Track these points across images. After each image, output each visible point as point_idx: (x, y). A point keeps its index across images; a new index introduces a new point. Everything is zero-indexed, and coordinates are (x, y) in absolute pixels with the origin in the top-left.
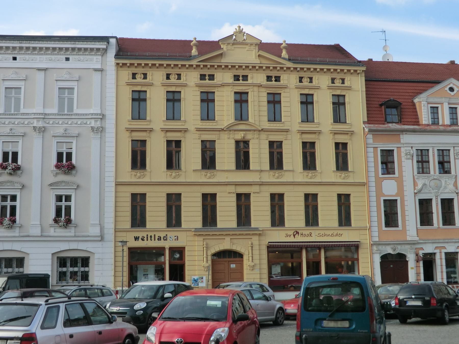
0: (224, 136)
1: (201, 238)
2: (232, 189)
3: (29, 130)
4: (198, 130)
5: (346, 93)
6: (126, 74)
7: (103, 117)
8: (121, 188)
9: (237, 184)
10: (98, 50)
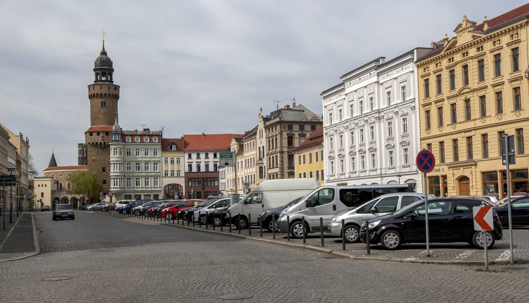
0: (458, 99)
1: (451, 169)
2: (463, 134)
3: (393, 114)
4: (449, 98)
5: (519, 45)
6: (421, 70)
7: (415, 99)
8: (422, 142)
9: (466, 131)
10: (409, 59)
